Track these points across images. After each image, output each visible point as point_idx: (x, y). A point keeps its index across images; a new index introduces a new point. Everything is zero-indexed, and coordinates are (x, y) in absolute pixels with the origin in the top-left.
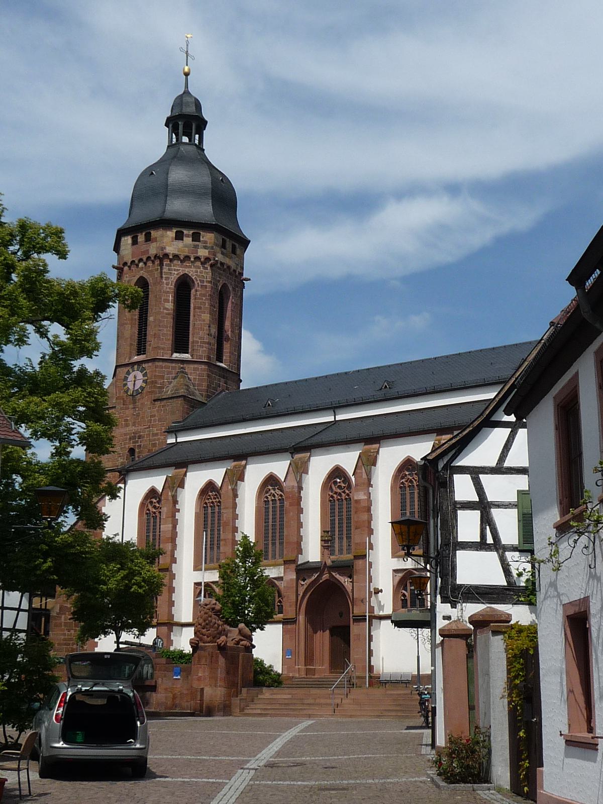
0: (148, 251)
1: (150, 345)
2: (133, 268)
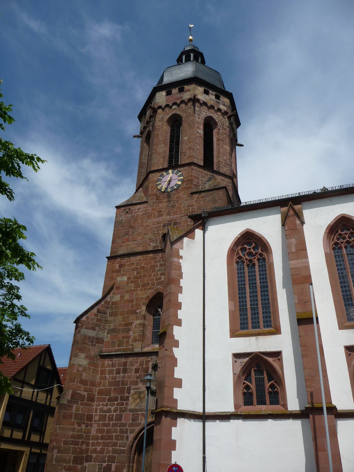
0: (182, 97)
2: (167, 110)
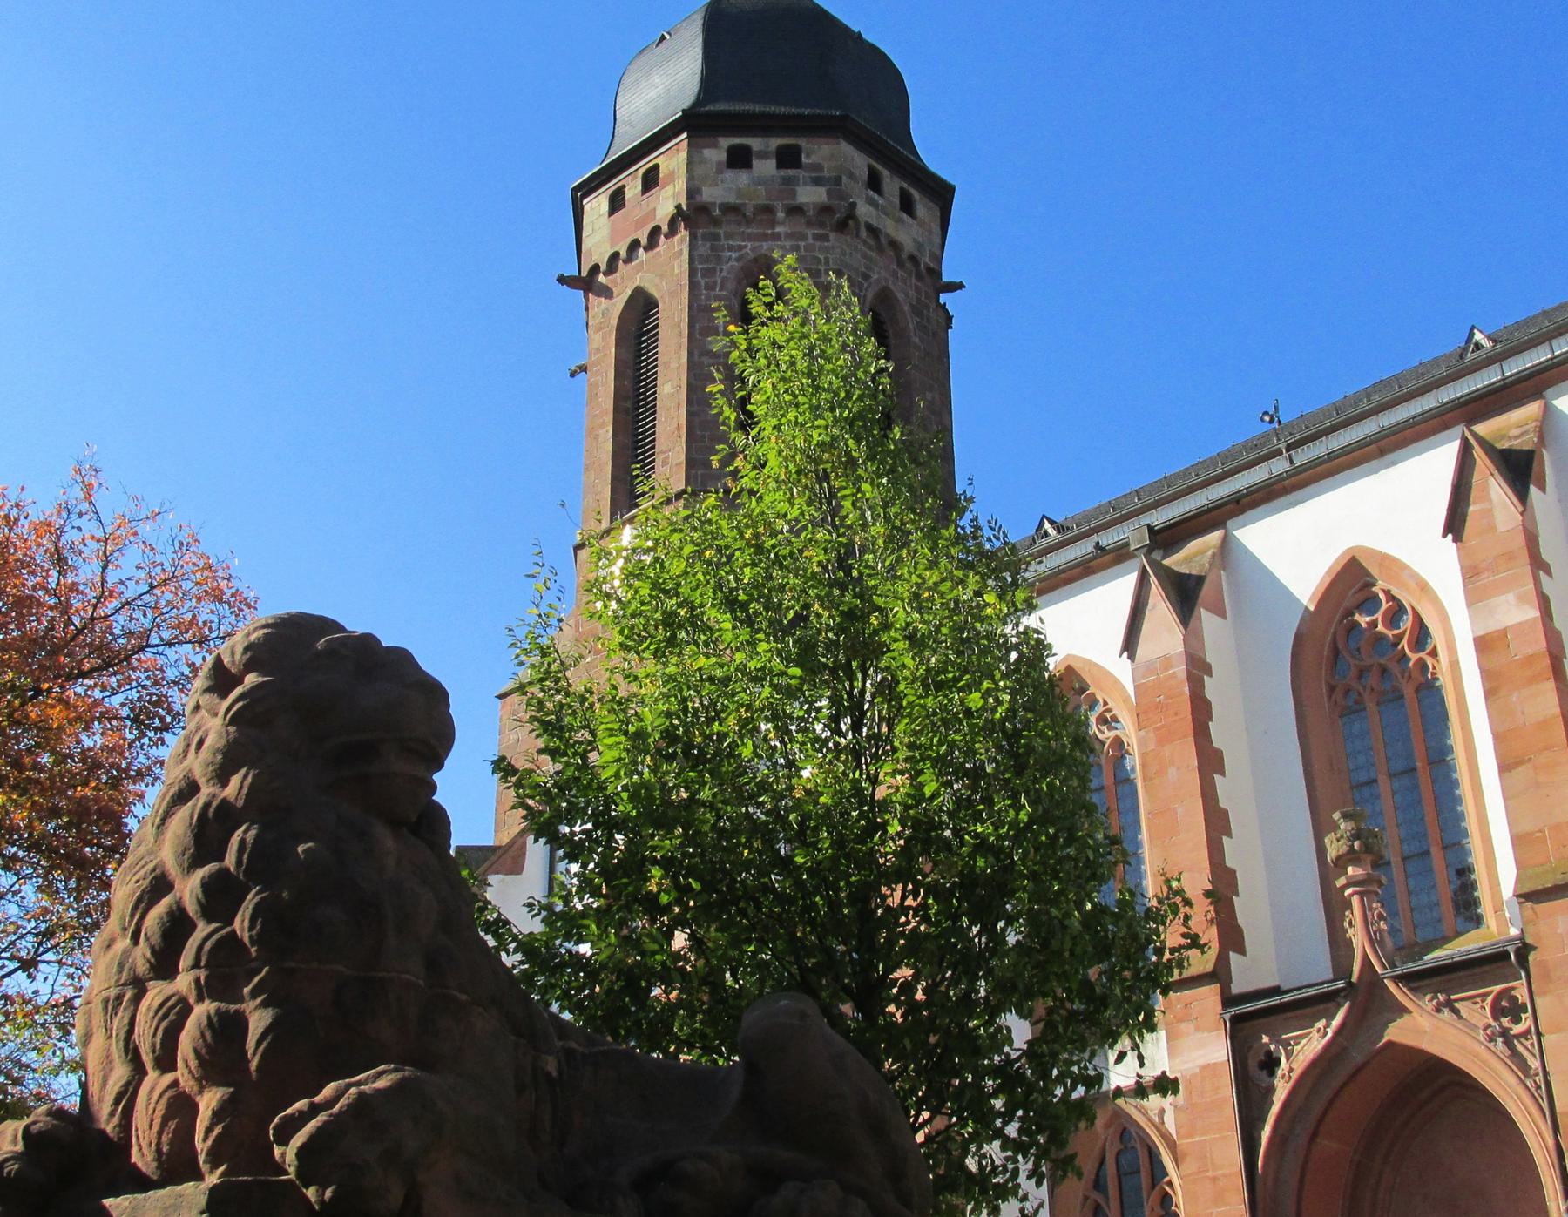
1: (665, 463)
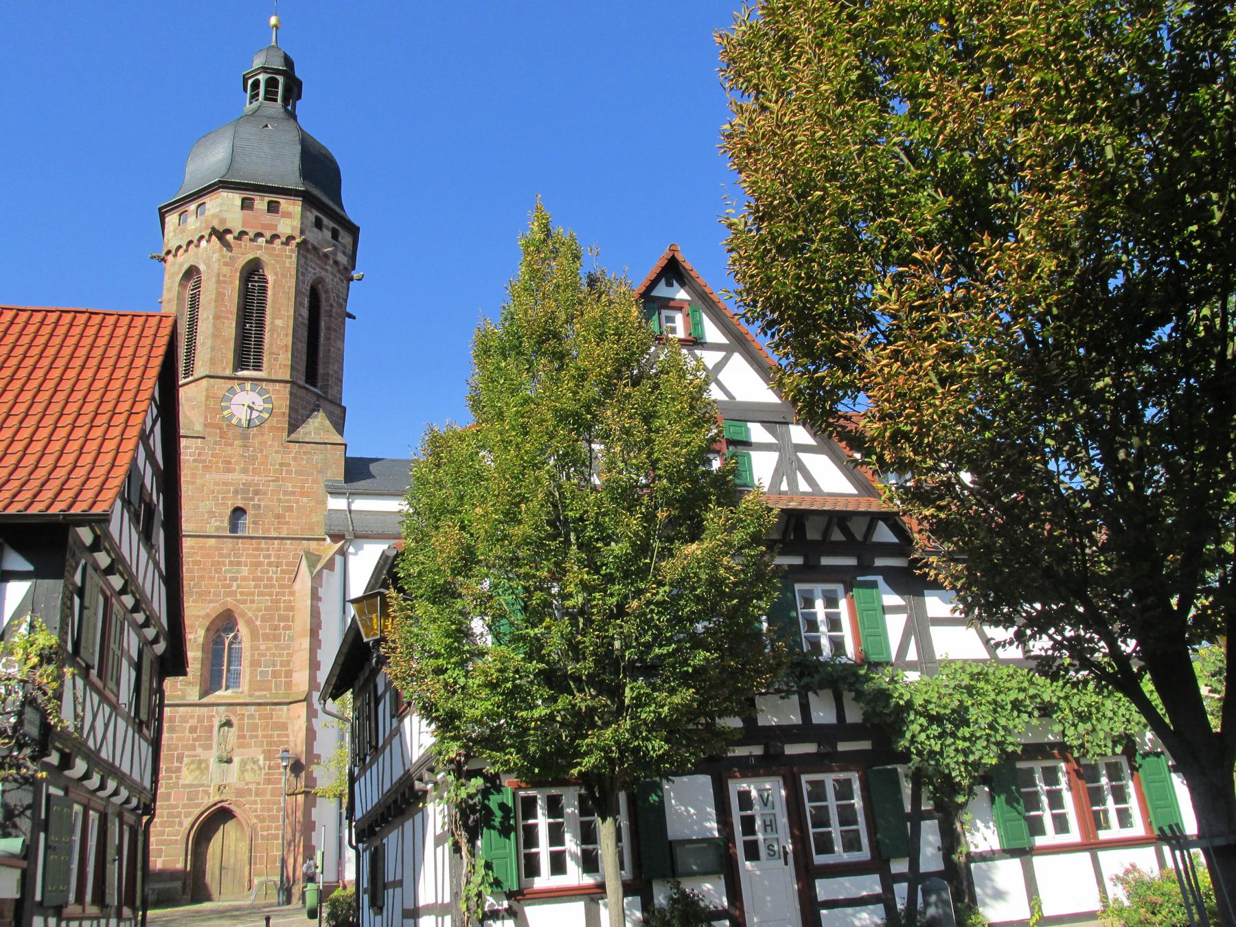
0: (275, 227)
